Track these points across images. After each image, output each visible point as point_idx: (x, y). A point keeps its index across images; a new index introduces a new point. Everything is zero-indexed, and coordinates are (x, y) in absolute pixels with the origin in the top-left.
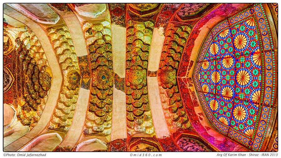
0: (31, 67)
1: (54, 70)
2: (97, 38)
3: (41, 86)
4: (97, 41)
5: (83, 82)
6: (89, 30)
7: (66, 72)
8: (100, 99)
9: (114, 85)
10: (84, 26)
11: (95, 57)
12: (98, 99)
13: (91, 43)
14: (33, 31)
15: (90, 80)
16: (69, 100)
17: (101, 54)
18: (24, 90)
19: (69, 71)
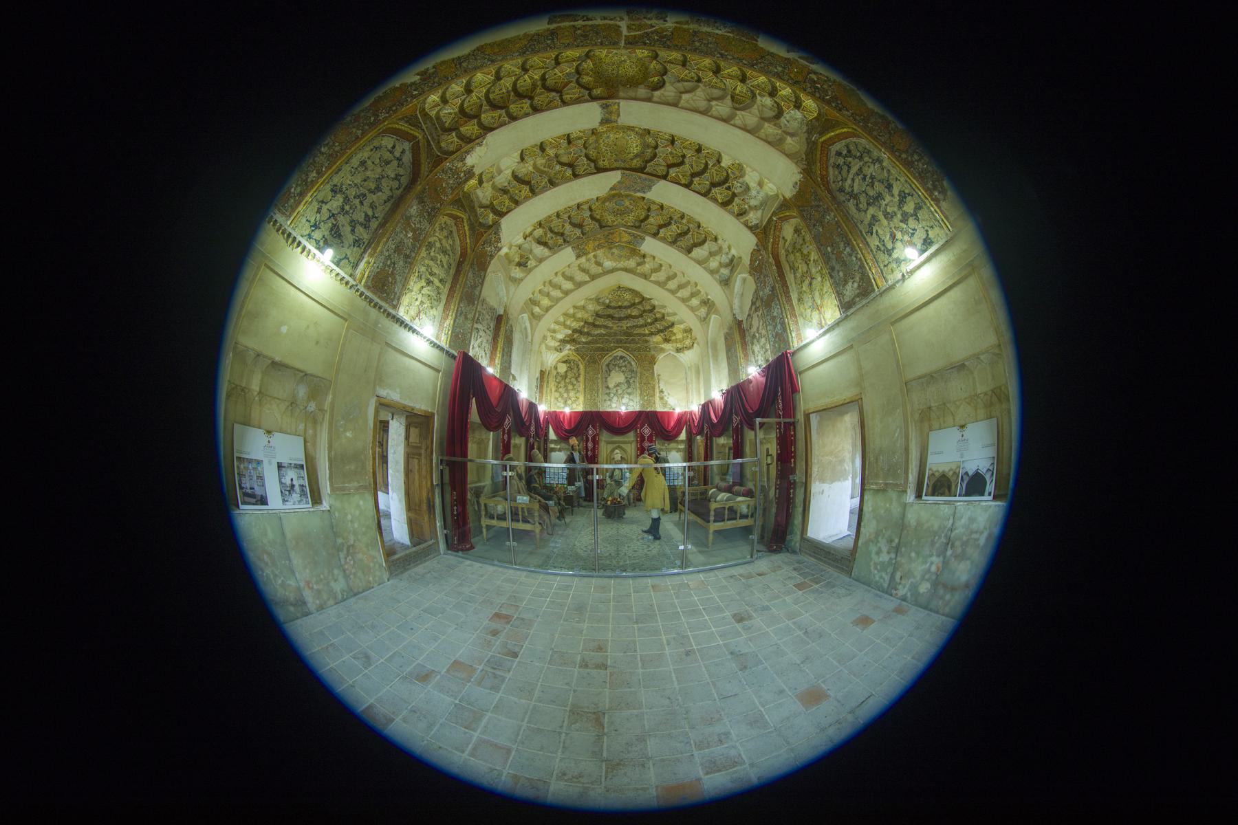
0: (600, 322)
1: (605, 284)
2: (533, 242)
3: (633, 305)
4: (538, 240)
5: (629, 243)
6: (522, 264)
7: (608, 264)
8: (669, 224)
9: (639, 194)
10: (517, 277)
11: (573, 231)
12: (669, 228)
13: (546, 250)
14: (542, 335)
15: (624, 231)
16: (663, 268)
17: (565, 221)
18: (637, 334)
19: (605, 260)
